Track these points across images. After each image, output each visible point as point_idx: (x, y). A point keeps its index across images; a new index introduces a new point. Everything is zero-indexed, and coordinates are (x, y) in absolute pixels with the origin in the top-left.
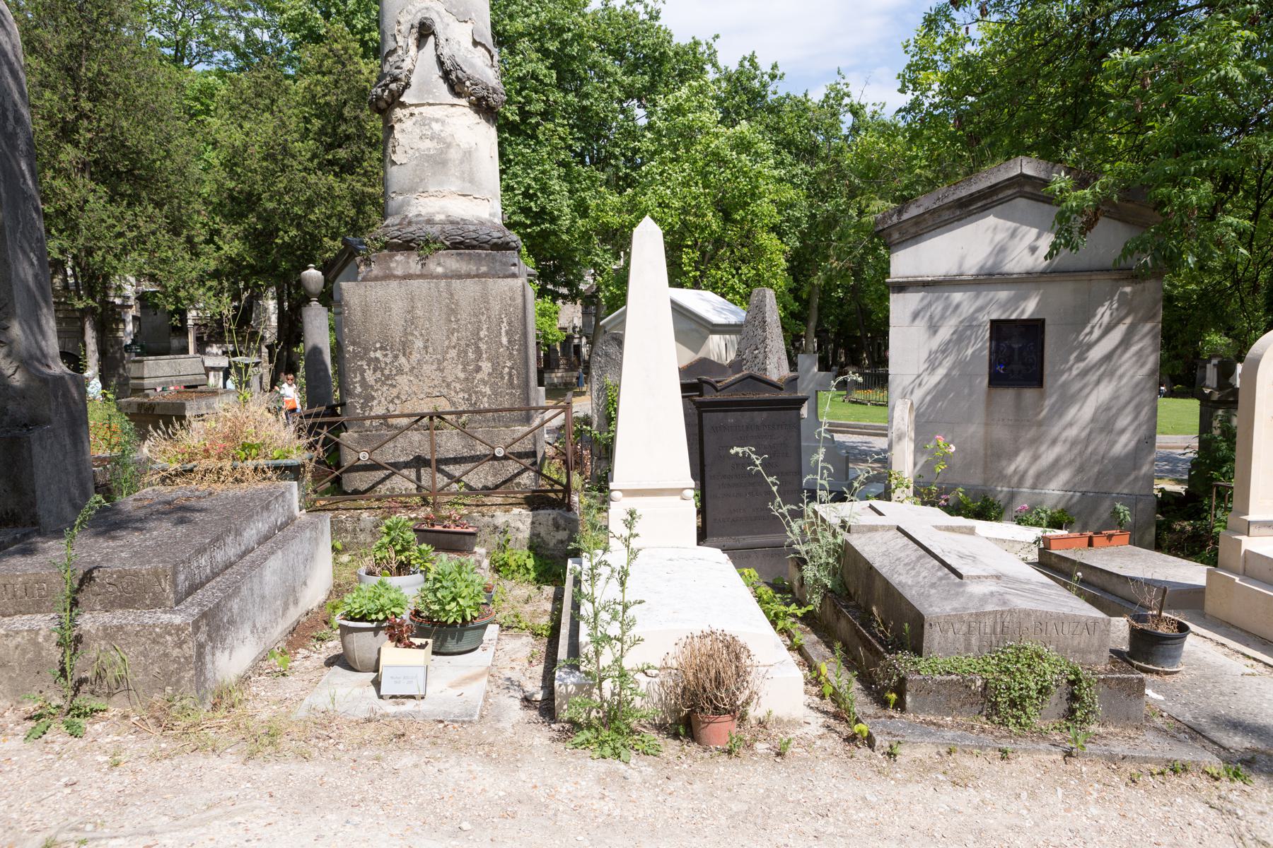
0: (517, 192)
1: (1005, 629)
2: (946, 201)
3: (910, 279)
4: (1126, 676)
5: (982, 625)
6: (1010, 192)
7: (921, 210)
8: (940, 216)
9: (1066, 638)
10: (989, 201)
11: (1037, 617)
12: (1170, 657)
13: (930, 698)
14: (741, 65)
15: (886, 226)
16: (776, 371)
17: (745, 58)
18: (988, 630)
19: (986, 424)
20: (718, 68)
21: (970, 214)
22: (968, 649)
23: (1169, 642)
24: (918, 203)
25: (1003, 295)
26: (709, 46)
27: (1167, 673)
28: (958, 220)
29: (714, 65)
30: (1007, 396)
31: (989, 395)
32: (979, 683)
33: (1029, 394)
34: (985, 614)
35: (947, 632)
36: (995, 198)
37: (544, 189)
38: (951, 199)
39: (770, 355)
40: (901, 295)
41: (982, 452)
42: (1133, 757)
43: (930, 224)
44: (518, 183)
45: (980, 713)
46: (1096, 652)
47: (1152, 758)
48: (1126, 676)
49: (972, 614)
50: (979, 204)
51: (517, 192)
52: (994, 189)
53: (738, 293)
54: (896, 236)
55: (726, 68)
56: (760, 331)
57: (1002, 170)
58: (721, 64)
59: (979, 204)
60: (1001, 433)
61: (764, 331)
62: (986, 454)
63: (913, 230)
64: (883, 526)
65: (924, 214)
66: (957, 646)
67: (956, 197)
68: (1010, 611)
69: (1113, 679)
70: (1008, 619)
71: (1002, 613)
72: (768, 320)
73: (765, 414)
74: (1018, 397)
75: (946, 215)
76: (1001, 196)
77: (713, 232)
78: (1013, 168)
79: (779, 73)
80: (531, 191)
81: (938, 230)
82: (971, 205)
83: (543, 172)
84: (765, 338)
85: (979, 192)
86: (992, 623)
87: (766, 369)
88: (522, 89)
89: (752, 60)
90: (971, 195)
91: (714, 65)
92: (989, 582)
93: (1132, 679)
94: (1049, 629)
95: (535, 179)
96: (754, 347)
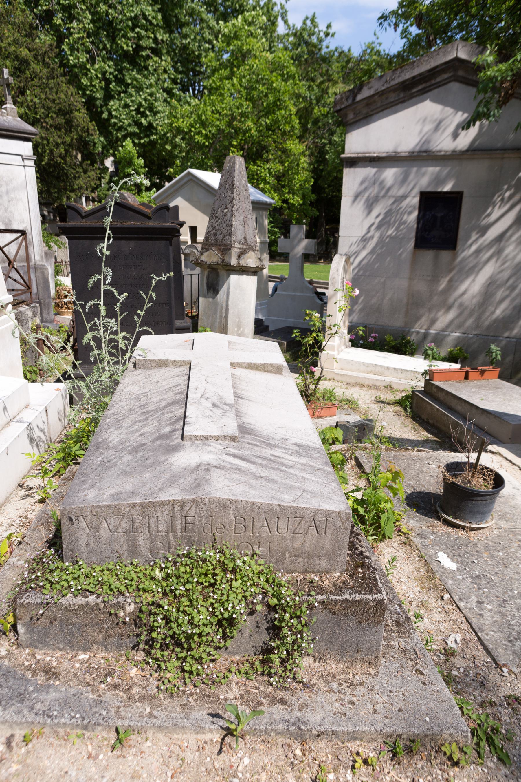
0: (132, 108)
1: (190, 526)
2: (393, 83)
3: (360, 155)
4: (358, 597)
5: (152, 520)
6: (446, 76)
7: (372, 92)
8: (387, 98)
9: (283, 538)
10: (428, 84)
11: (237, 509)
12: (479, 513)
13: (55, 629)
14: (304, 23)
15: (343, 106)
16: (241, 227)
17: (307, 18)
18: (162, 527)
19: (411, 279)
20: (288, 25)
21: (412, 96)
22: (134, 551)
23: (479, 498)
24: (370, 85)
25: (432, 170)
26: (282, 7)
27: (473, 529)
28: (403, 102)
29: (286, 22)
30: (428, 255)
31: (414, 255)
32: (130, 608)
33: (445, 255)
34: (155, 505)
35: (97, 528)
36: (433, 82)
37: (151, 108)
38: (397, 81)
39: (236, 213)
40: (352, 169)
41: (405, 300)
42: (334, 733)
43: (379, 105)
44: (132, 101)
45: (133, 648)
46: (328, 556)
47: (364, 733)
48: (358, 597)
49: (134, 505)
50: (420, 87)
51: (132, 108)
52: (433, 72)
53: (269, 183)
54: (351, 116)
55: (294, 26)
56: (229, 193)
57: (441, 54)
58: (290, 22)
59: (420, 87)
60: (421, 286)
61: (232, 193)
62: (408, 303)
63: (365, 111)
64: (175, 361)
65: (373, 95)
66: (116, 548)
67: (401, 80)
68: (194, 501)
69: (337, 601)
70: (193, 512)
71: (183, 503)
72: (237, 183)
73: (132, 243)
74: (436, 257)
75: (392, 97)
76: (438, 79)
77: (251, 136)
78: (450, 52)
79: (331, 31)
80: (142, 110)
81: (385, 112)
82: (413, 88)
83: (151, 95)
84: (233, 199)
85: (420, 75)
86: (168, 518)
87: (231, 226)
88: (135, 26)
89: (313, 21)
90: (414, 78)
91: (286, 22)
92: (217, 446)
93: (367, 601)
94: (257, 525)
95: (145, 100)
96: (224, 207)
